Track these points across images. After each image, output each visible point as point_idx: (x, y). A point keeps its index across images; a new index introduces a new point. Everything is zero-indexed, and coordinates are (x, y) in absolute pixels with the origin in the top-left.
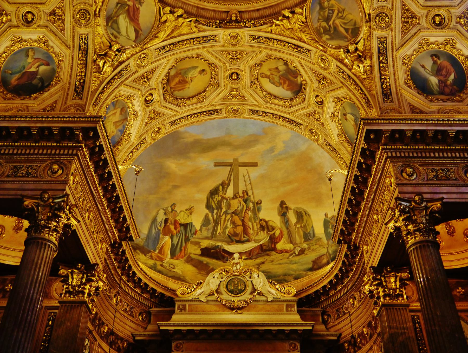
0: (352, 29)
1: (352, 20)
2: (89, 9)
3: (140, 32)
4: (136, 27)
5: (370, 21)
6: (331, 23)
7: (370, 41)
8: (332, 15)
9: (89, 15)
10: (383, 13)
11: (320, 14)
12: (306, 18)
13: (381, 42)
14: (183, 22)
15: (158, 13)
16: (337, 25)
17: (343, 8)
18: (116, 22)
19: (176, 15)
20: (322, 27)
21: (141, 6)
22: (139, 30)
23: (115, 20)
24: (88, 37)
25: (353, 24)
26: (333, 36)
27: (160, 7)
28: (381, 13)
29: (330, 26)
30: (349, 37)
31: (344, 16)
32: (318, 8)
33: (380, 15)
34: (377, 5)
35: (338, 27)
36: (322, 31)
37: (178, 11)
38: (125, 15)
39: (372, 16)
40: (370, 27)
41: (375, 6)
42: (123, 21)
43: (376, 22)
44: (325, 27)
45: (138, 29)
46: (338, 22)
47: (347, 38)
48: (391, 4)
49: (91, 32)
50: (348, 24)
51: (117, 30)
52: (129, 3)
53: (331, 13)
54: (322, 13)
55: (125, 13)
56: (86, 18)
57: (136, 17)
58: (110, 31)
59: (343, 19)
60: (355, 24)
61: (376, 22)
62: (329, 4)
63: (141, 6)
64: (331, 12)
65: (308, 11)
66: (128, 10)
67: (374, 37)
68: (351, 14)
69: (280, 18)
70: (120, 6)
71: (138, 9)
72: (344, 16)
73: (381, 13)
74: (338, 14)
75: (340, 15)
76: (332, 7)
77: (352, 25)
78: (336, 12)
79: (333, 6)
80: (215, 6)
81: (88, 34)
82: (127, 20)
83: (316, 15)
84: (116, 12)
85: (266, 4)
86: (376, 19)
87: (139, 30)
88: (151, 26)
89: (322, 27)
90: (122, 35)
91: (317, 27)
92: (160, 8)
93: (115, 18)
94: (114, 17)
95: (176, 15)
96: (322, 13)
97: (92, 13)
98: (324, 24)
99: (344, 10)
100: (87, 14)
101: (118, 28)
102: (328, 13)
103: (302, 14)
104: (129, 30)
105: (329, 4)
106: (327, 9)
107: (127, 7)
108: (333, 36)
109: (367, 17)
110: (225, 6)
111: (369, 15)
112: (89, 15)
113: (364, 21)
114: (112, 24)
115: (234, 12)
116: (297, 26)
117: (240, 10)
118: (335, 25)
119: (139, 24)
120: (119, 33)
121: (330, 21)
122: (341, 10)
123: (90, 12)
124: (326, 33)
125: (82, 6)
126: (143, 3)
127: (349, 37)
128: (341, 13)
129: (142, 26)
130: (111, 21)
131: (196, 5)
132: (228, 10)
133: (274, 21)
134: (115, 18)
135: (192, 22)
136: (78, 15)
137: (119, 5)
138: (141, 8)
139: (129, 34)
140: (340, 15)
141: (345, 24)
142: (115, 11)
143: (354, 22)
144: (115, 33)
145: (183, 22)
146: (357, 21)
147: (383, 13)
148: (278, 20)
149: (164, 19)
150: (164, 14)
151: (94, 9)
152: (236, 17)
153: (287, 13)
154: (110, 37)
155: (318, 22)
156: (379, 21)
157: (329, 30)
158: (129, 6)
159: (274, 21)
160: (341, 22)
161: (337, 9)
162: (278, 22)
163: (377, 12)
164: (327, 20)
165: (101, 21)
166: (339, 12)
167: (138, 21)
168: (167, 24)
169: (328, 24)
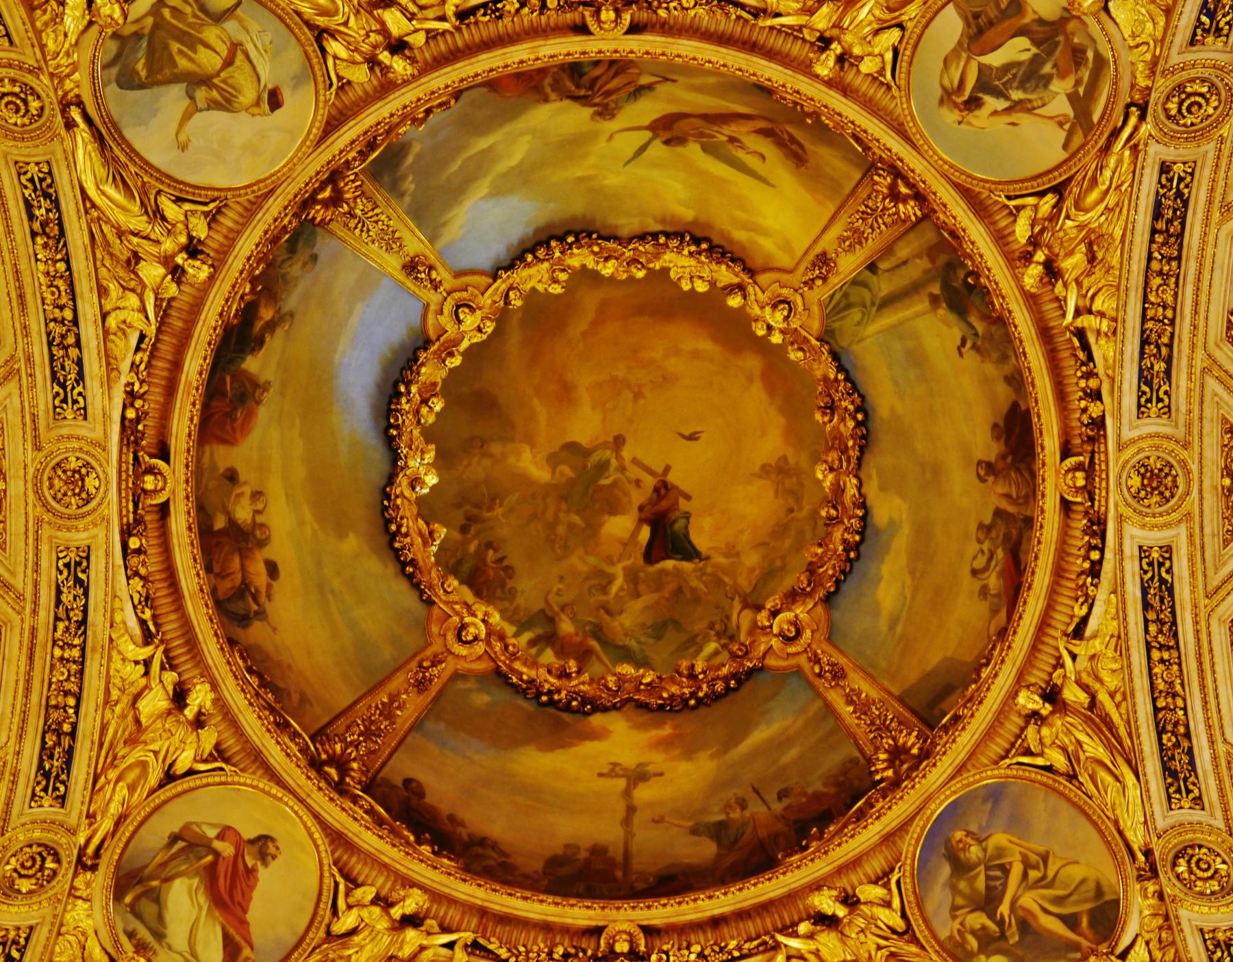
0: (1092, 913)
1: (1083, 881)
2: (62, 839)
3: (247, 952)
4: (232, 931)
5: (1154, 874)
6: (1004, 909)
7: (1173, 943)
8: (1005, 885)
9: (58, 860)
10: (1200, 847)
11: (954, 890)
12: (904, 916)
13: (1217, 945)
14: (422, 948)
15: (327, 897)
16: (1028, 911)
17: (1041, 849)
18: (156, 898)
19: (396, 912)
20: (973, 932)
21: (265, 864)
22: (243, 943)
23: (153, 889)
24: (27, 939)
25: (1092, 894)
26: (1019, 952)
27: (339, 879)
28: (1192, 847)
29: (1001, 923)
30: (1085, 943)
31: (1051, 874)
32: (946, 870)
33: (1190, 851)
34: (1170, 821)
35: (1034, 916)
36: (973, 943)
37: (403, 899)
38: (196, 881)
39: (1157, 854)
40: (1161, 896)
41: (1161, 824)
42: (184, 900)
43: (1178, 876)
44: (984, 928)
45: (238, 938)
46: (1029, 900)
47: (1076, 947)
48: (1219, 814)
49: (49, 919)
50: (1073, 898)
51: (154, 924)
52: (218, 845)
53: (997, 878)
54: (963, 885)
55: (197, 873)
56: (42, 868)
57: (239, 897)
58: (124, 920)
59: (1050, 885)
60: (1099, 891)
61: (1178, 876)
62: (985, 850)
63: (265, 864)
64: (998, 873)
65: (907, 886)
66: (211, 870)
67: (1185, 925)
68: (1076, 862)
69: (804, 928)
70: (182, 850)
71: (251, 872)
72: (1051, 874)
73: (1192, 847)
74: (1025, 875)
75: (1034, 874)
76: (1000, 857)
77: (1086, 901)
78: (1017, 870)
79: (1000, 852)
80: (552, 909)
81: (31, 928)
82: (202, 899)
83: (939, 897)
84: (163, 865)
85: (746, 900)
86: (1174, 865)
87: (243, 943)
88: (293, 940)
89: (973, 932)
90: (170, 948)
91: (951, 937)
92: (337, 884)
93: (155, 883)
94: (151, 878)
95: (396, 912)
96: (963, 885)
97: (69, 856)
98: (978, 920)
99: (1045, 858)
100: (50, 859)
101: (161, 918)
102: (988, 878)
103: (888, 904)
104: (200, 935)
105: (985, 850)
106: (982, 868)
107: (210, 858)
108: (1019, 952)
109: (1141, 858)
110: (591, 912)
111: (1148, 853)
112: (58, 860)
113: (1132, 873)
114: (137, 898)
115: (625, 927)
116: (872, 942)
117: (645, 923)
118: (1021, 913)
119: (243, 924)
120: (159, 936)
121: (1000, 902)
122: (1034, 858)
123: (62, 854)
124: (993, 946)
125: (37, 834)
126: (274, 857)
127: (1085, 943)
128: (1036, 867)
129: (256, 933)
130: (138, 890)
131: (479, 903)
132: (601, 923)
133: (780, 938)
134: (155, 883)
135: (457, 948)
136: (13, 860)
137: (181, 844)
138: (262, 873)
139: (199, 949)
140: (1034, 874)
141: (1058, 900)
142: (159, 859)
143: (1091, 885)
144: (144, 934)
145: (422, 948)
146: (1104, 882)
147: (1200, 847)
148: (795, 935)
149: (348, 921)
150: (350, 907)
151: (82, 841)
152: (632, 942)
153: (826, 902)
154: (116, 942)
155: (954, 917)
156: (1191, 872)
157: (1003, 936)
158: (217, 854)
159: (780, 938)
160: (1043, 897)
161: (1019, 857)
162: (794, 943)
163: (1175, 841)
164: (988, 903)
165: (99, 882)
166: (1027, 865)
167: (245, 911)
168: (356, 939)
169: (991, 916)
